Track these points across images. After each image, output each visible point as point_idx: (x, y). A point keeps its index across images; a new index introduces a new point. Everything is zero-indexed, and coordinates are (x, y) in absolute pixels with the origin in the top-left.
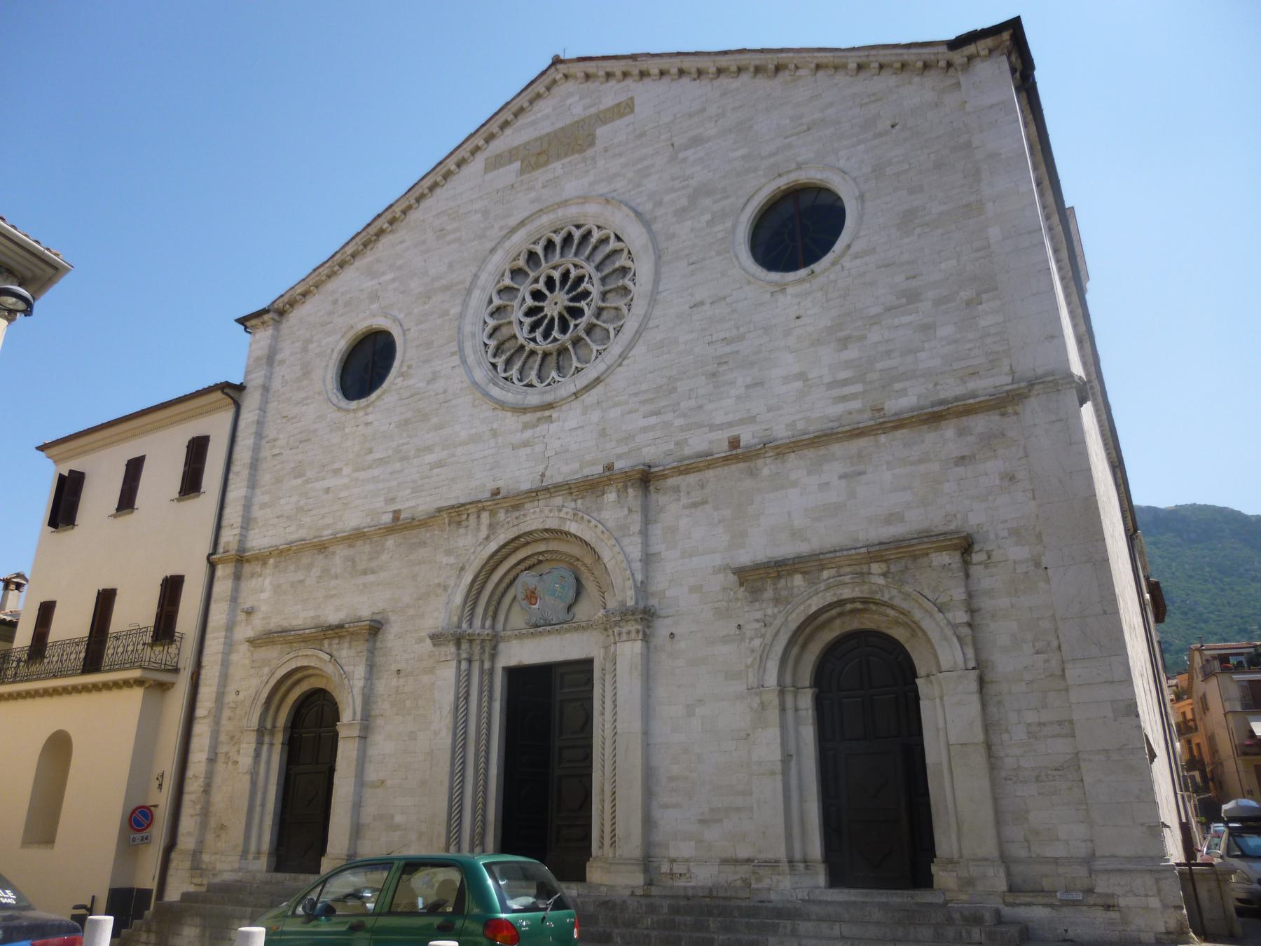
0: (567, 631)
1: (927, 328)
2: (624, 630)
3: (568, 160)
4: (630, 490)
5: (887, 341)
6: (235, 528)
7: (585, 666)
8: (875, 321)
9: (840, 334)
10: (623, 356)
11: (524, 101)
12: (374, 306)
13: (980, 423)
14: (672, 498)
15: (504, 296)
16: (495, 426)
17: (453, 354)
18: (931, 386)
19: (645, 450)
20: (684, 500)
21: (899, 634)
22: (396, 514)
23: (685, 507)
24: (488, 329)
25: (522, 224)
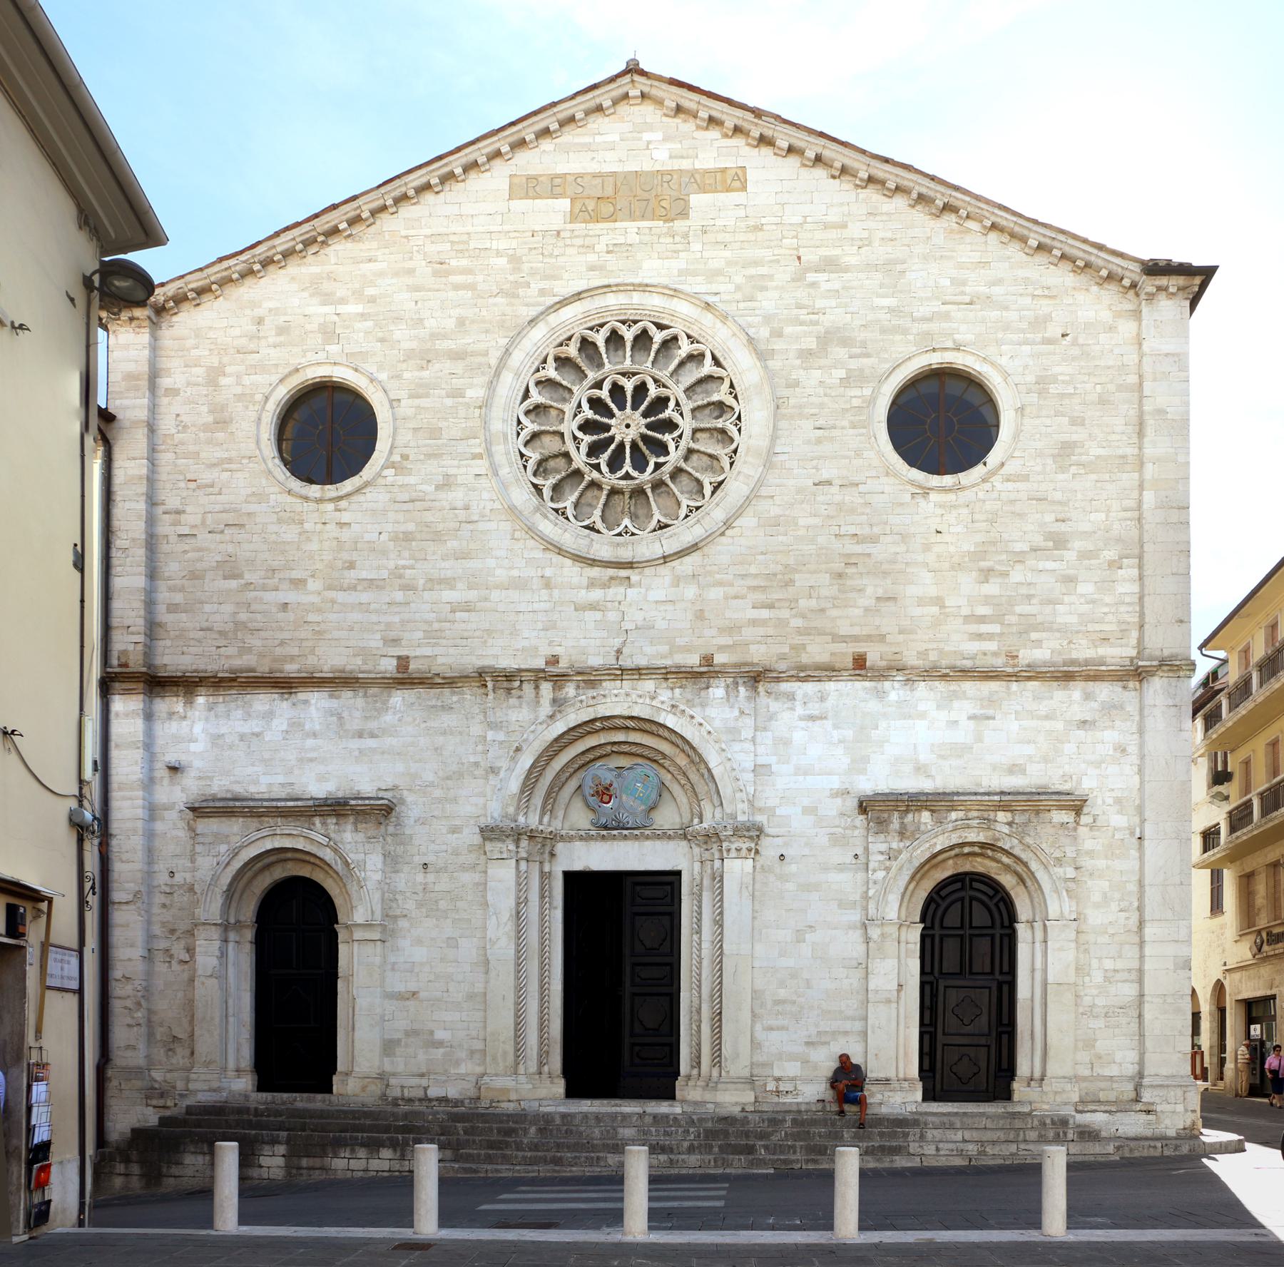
0: (647, 838)
1: (1070, 580)
2: (733, 847)
3: (645, 224)
4: (742, 689)
5: (1030, 584)
6: (133, 633)
7: (673, 878)
8: (1019, 558)
9: (984, 564)
10: (728, 524)
11: (577, 108)
12: (334, 349)
13: (1105, 691)
14: (786, 706)
15: (547, 393)
16: (548, 572)
17: (476, 456)
18: (1065, 643)
19: (753, 648)
20: (800, 710)
21: (1007, 880)
22: (403, 662)
23: (801, 719)
24: (525, 434)
25: (578, 296)
